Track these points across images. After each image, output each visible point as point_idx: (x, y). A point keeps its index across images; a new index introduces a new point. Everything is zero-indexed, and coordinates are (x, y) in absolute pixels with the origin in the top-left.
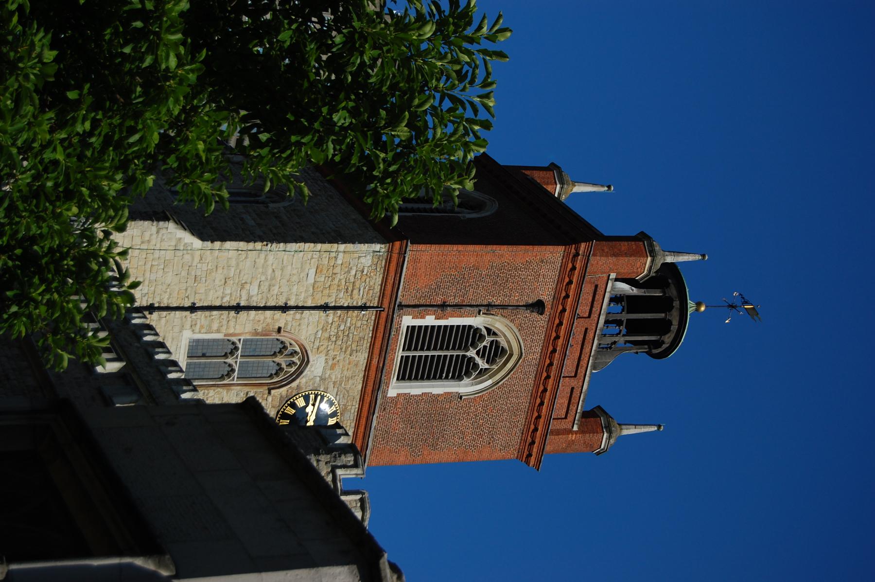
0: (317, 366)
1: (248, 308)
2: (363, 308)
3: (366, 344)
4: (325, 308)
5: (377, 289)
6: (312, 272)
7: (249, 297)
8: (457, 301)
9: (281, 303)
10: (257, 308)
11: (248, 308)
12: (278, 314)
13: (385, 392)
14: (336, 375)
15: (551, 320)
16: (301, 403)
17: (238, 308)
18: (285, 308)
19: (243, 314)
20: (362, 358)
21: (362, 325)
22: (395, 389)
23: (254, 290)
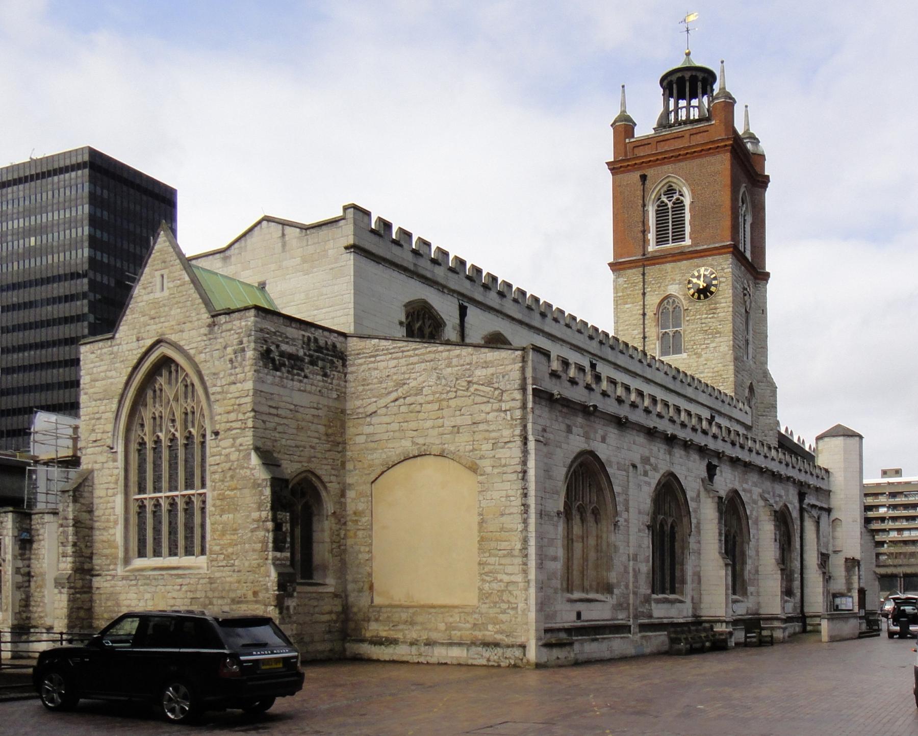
0: (673, 289)
1: (644, 332)
2: (644, 274)
3: (663, 266)
4: (644, 294)
5: (634, 270)
6: (627, 306)
7: (639, 333)
8: (640, 225)
9: (641, 317)
10: (644, 328)
11: (644, 332)
12: (647, 317)
13: (689, 246)
14: (678, 277)
15: (650, 167)
16: (692, 291)
17: (644, 338)
18: (644, 314)
19: (647, 335)
20: (669, 266)
21: (651, 271)
22: (688, 242)
23: (636, 332)
